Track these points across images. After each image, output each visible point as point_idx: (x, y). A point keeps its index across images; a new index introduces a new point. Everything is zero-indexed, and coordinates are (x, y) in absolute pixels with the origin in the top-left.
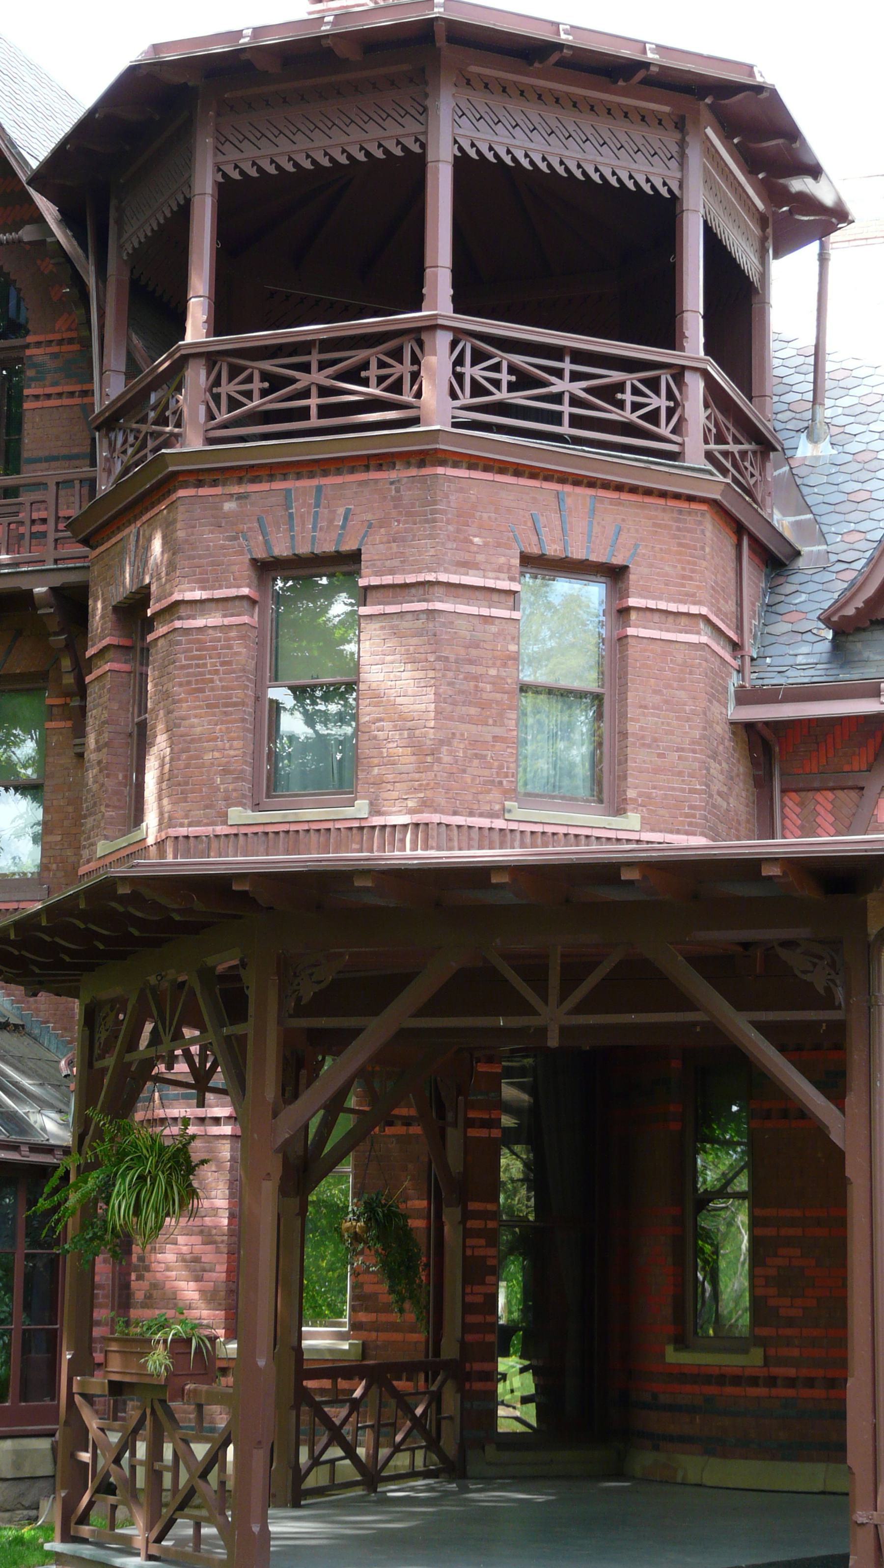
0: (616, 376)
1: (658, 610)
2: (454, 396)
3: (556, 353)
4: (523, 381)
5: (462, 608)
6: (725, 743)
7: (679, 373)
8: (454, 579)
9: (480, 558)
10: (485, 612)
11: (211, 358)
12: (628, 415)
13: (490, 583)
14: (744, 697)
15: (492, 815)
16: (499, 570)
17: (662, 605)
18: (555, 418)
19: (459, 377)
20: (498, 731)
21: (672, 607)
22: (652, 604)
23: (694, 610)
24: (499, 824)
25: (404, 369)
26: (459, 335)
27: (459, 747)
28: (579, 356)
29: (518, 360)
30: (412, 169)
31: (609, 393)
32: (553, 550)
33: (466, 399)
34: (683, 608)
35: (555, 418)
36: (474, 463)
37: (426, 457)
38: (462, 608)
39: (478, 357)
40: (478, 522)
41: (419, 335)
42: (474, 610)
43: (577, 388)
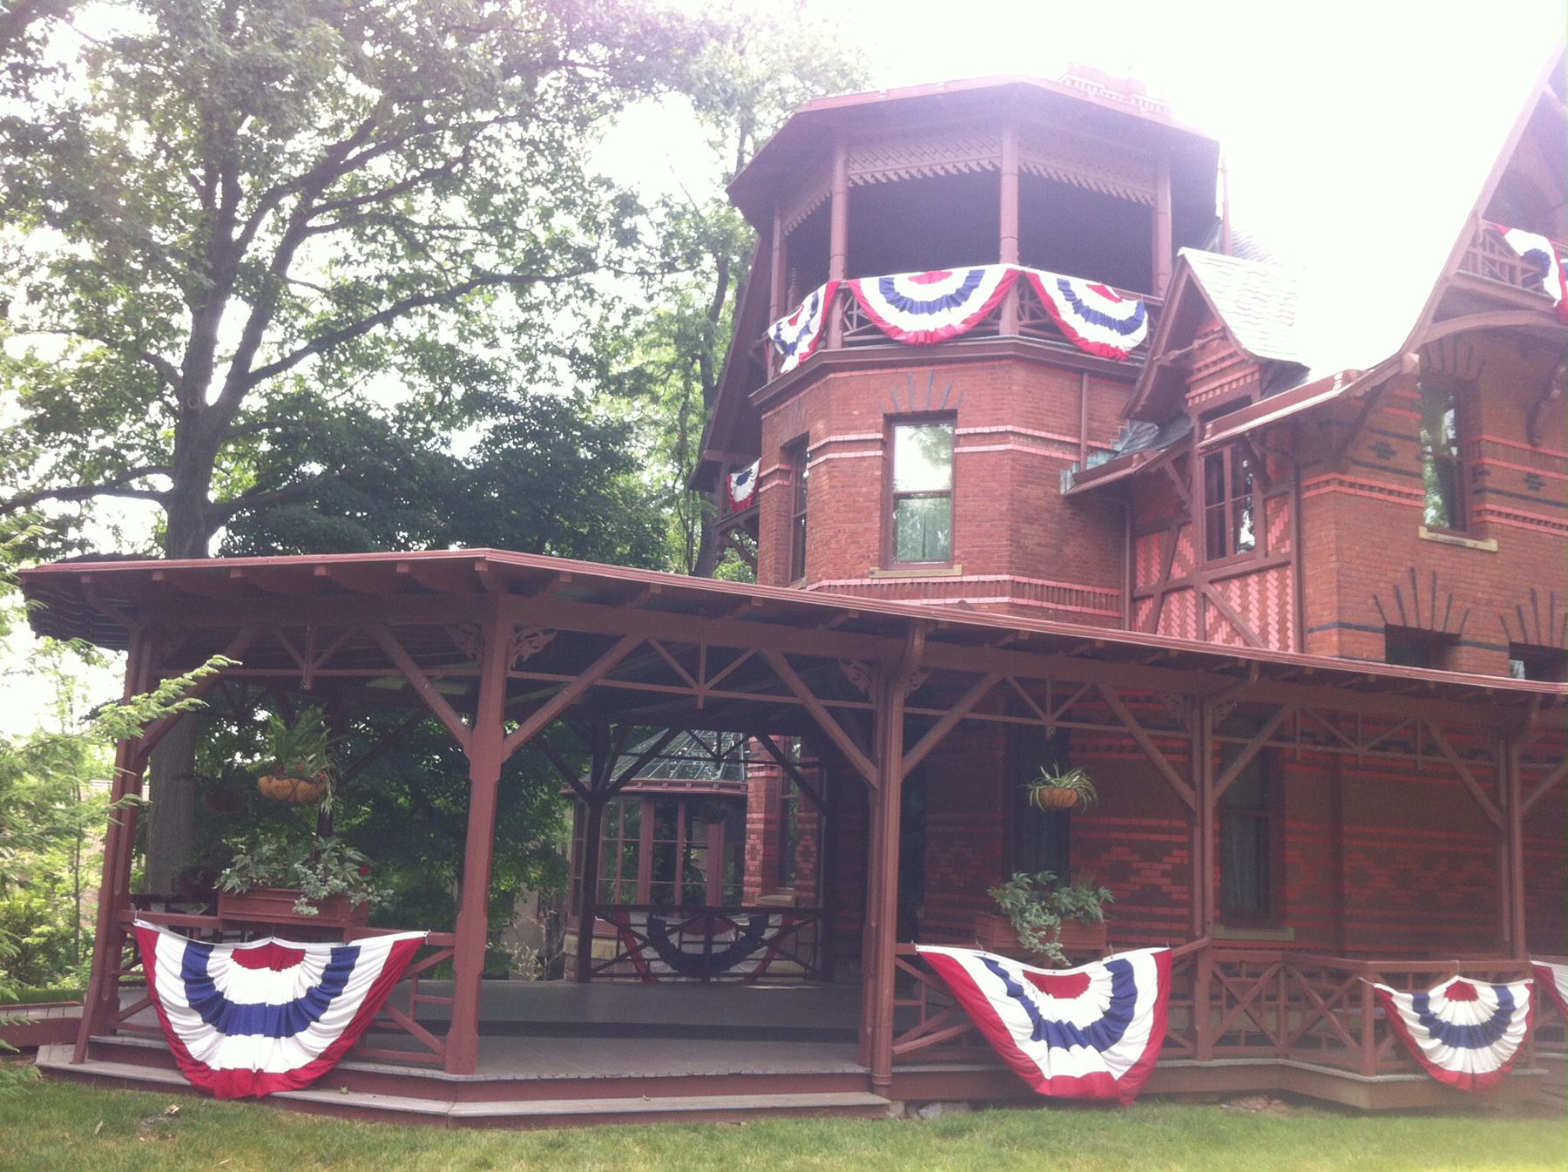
1: (976, 434)
2: (845, 328)
5: (844, 455)
8: (840, 438)
9: (857, 423)
10: (859, 454)
13: (862, 437)
15: (863, 576)
16: (870, 427)
17: (979, 430)
19: (850, 318)
20: (867, 525)
21: (986, 430)
22: (971, 430)
23: (1002, 429)
24: (867, 582)
27: (843, 538)
34: (994, 429)
38: (844, 455)
42: (852, 455)
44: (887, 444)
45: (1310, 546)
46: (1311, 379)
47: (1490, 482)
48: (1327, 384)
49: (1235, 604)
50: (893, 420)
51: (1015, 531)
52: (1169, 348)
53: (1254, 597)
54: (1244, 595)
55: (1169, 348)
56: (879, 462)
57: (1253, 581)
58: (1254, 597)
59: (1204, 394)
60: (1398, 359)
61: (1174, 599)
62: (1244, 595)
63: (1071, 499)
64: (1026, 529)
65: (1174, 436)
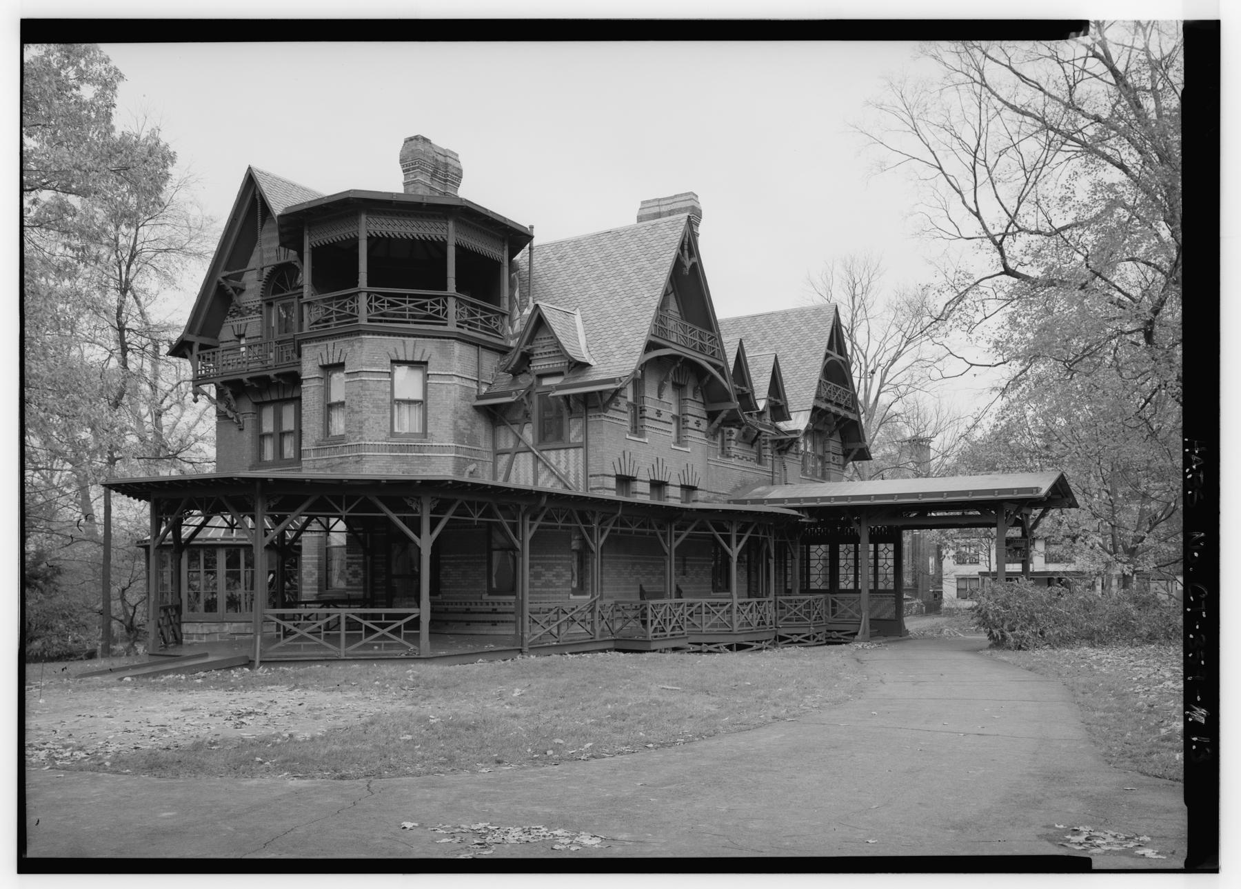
0: (425, 301)
3: (404, 295)
4: (392, 304)
6: (472, 412)
7: (446, 298)
11: (309, 303)
12: (429, 313)
14: (479, 398)
18: (404, 316)
25: (355, 305)
26: (369, 294)
28: (411, 296)
29: (390, 299)
30: (355, 242)
31: (422, 307)
32: (402, 358)
33: (373, 312)
35: (404, 316)
36: (374, 333)
37: (359, 333)
39: (377, 299)
40: (369, 352)
41: (357, 294)
43: (411, 306)
44: (391, 374)
45: (591, 442)
46: (592, 371)
47: (647, 414)
48: (612, 381)
49: (553, 461)
50: (396, 362)
51: (455, 422)
52: (527, 344)
53: (563, 459)
54: (558, 457)
55: (527, 344)
56: (389, 384)
57: (562, 452)
58: (563, 459)
59: (538, 365)
60: (635, 372)
61: (521, 455)
62: (558, 457)
63: (476, 408)
64: (460, 422)
65: (524, 381)
